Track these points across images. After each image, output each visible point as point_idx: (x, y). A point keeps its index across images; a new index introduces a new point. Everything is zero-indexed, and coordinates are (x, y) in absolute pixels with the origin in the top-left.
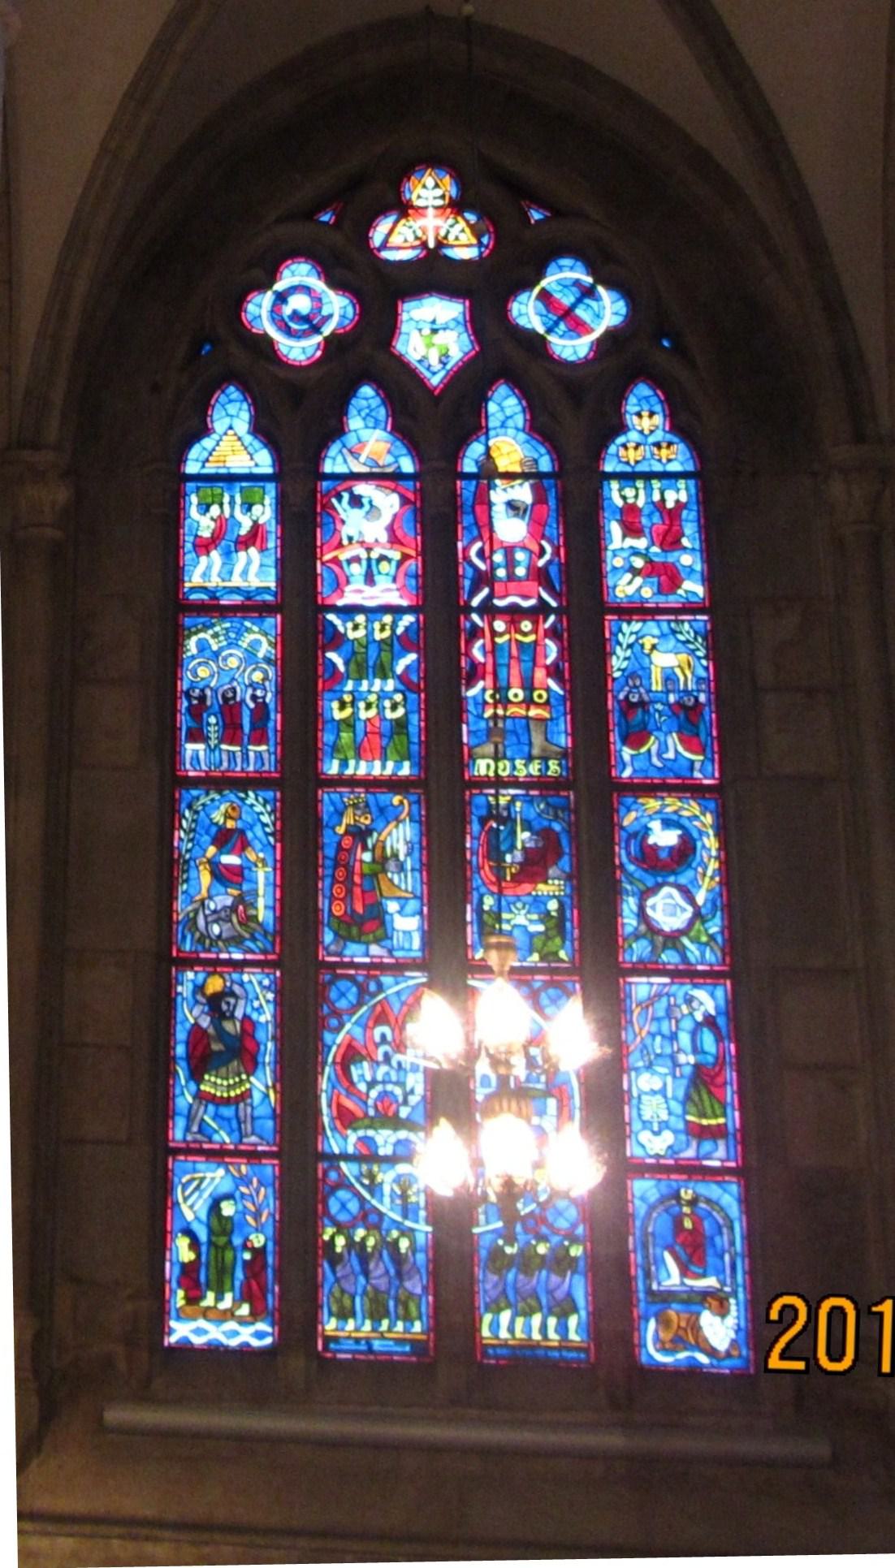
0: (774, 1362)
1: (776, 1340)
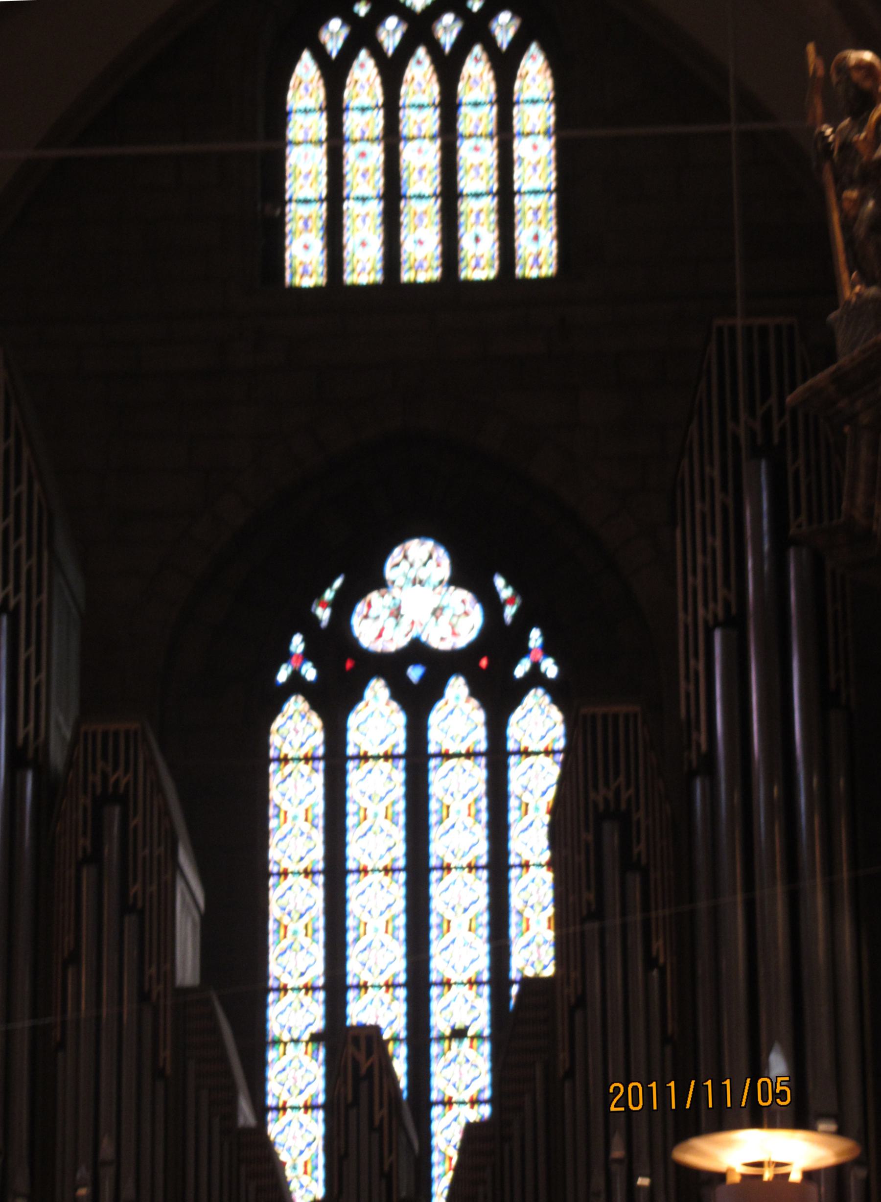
0: (613, 1109)
1: (613, 1100)
